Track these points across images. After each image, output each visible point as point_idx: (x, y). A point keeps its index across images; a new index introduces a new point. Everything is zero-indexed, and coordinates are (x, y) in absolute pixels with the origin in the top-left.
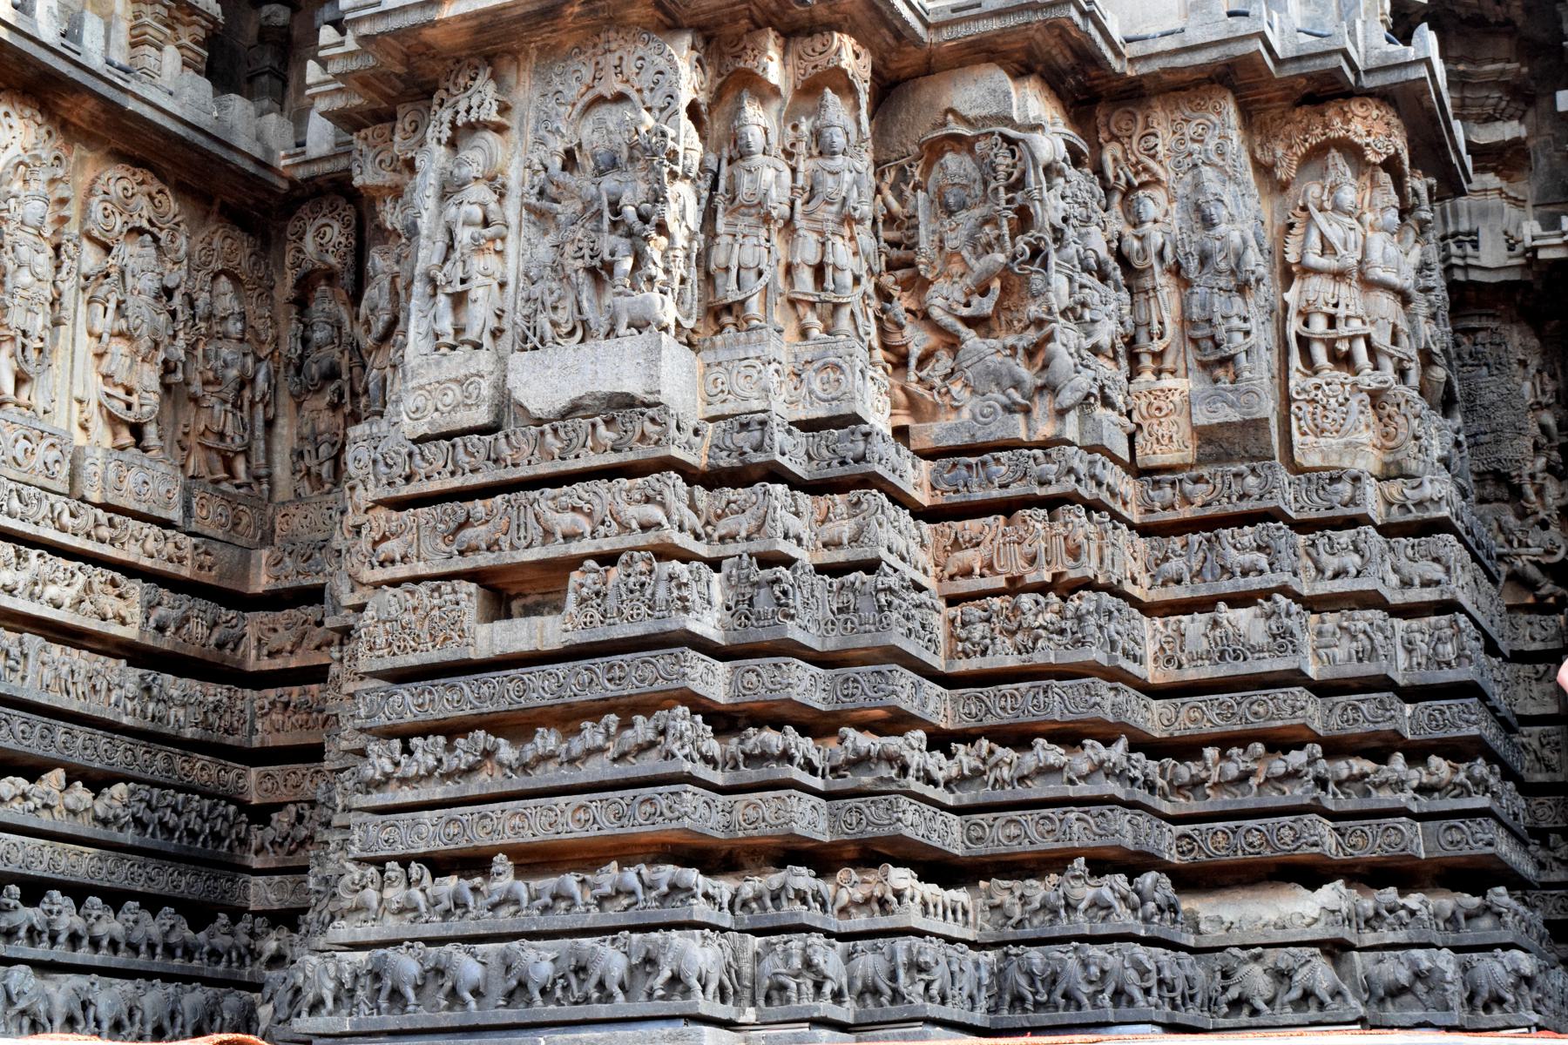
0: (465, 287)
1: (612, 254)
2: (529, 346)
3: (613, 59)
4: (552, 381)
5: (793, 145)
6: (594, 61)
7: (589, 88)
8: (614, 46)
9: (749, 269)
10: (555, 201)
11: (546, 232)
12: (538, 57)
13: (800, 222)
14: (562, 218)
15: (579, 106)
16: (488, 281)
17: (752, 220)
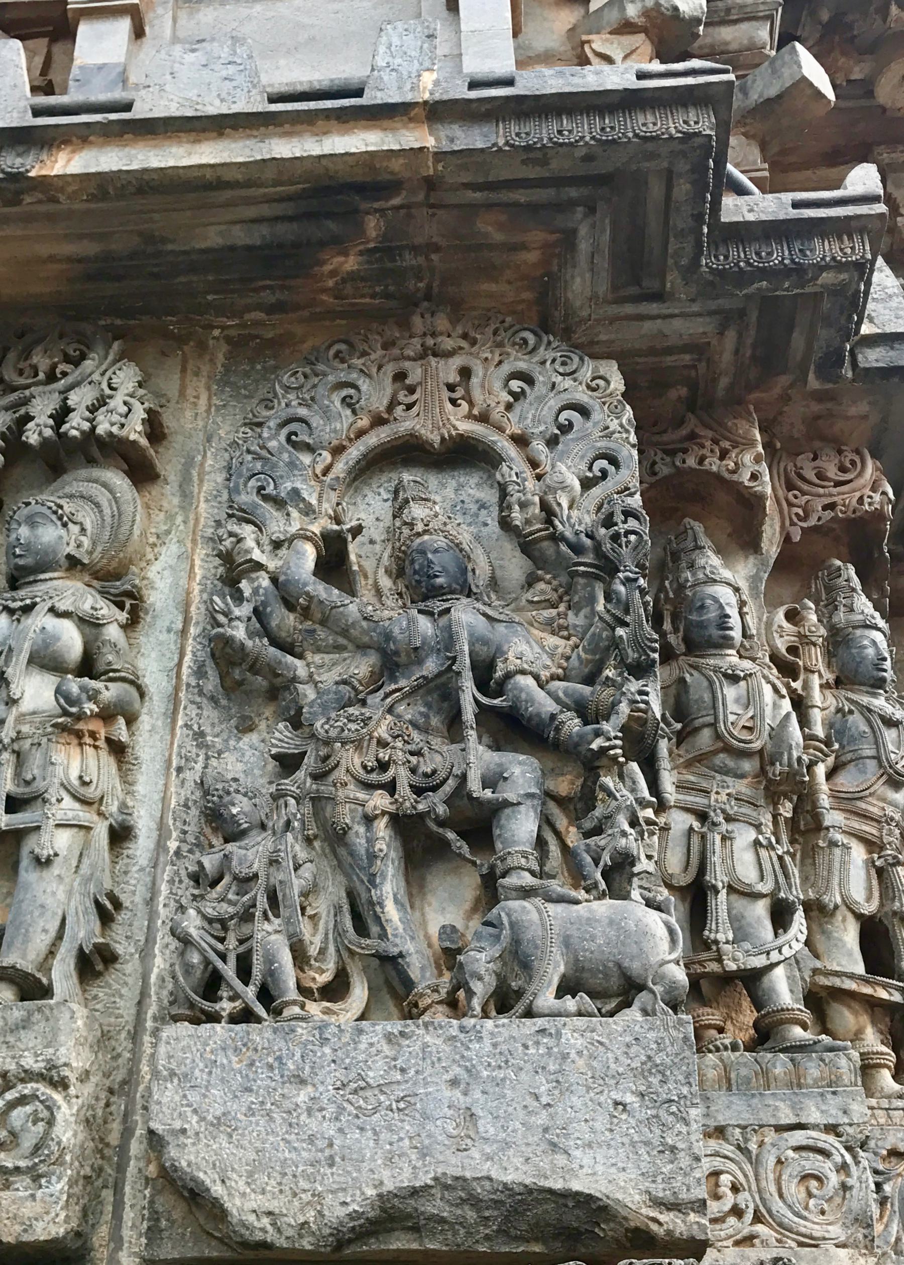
0: (20, 819)
1: (487, 783)
2: (226, 1006)
3: (449, 371)
4: (313, 1124)
5: (793, 650)
6: (390, 369)
7: (379, 421)
8: (448, 344)
9: (756, 896)
10: (289, 648)
11: (246, 727)
12: (229, 357)
13: (833, 818)
14: (308, 692)
15: (354, 452)
16: (85, 816)
17: (741, 787)
